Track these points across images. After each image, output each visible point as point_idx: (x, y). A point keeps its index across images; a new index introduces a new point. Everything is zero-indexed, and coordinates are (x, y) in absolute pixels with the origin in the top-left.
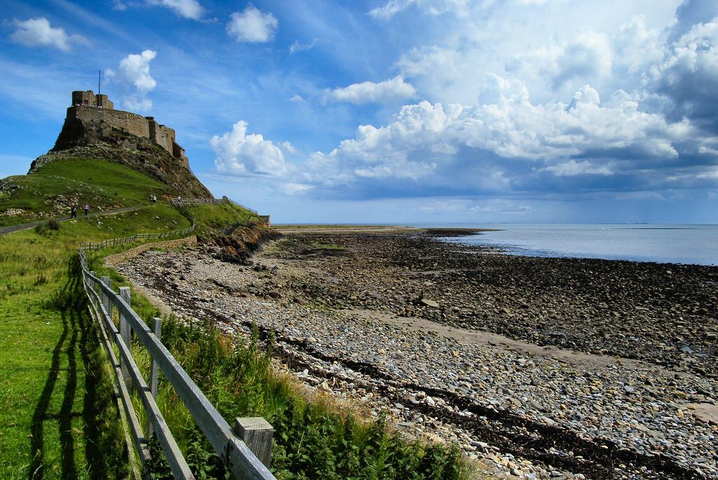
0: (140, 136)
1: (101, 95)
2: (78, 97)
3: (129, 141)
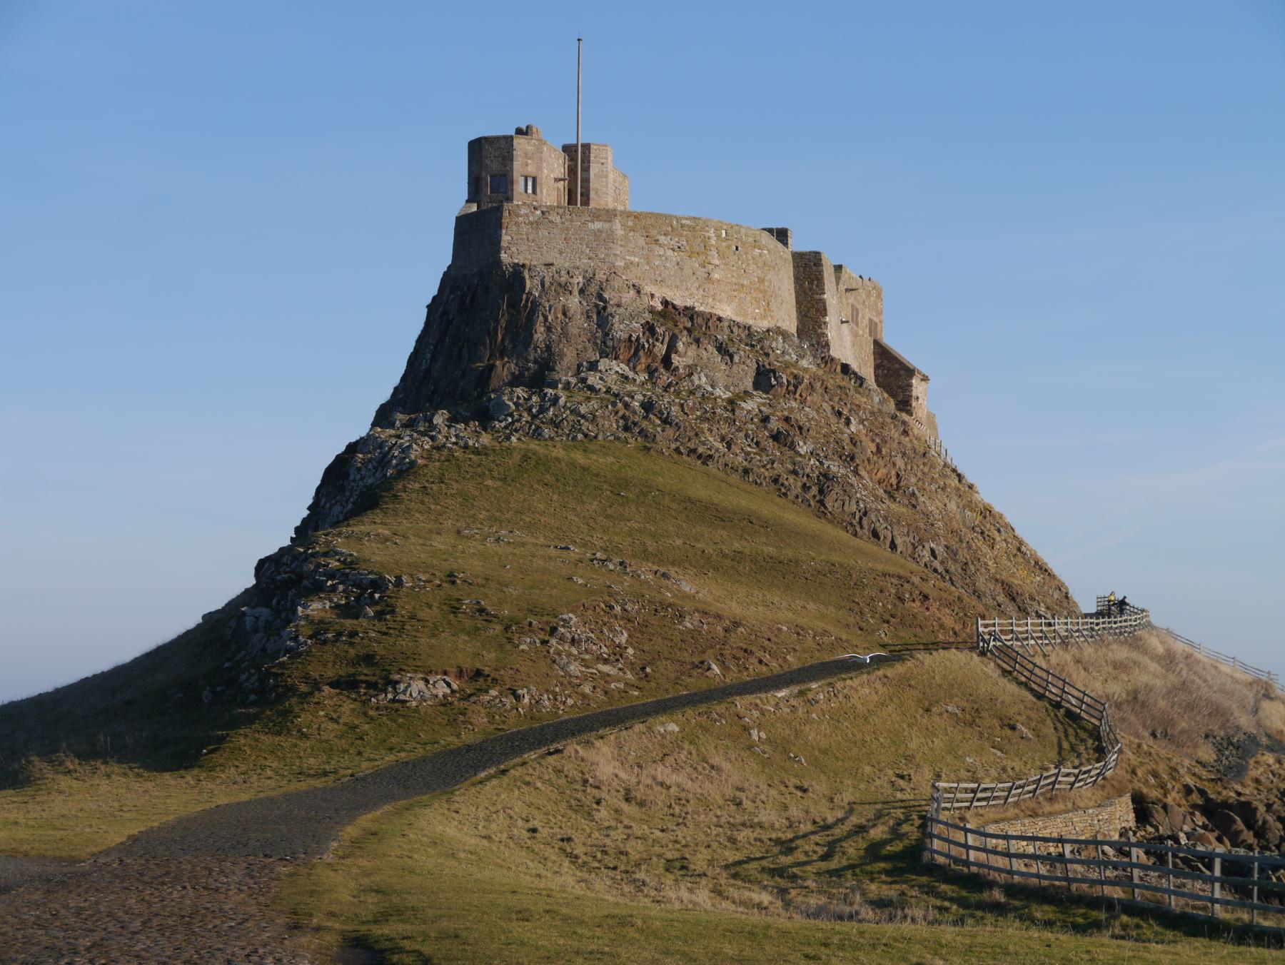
0: (762, 325)
1: (586, 147)
2: (493, 165)
3: (722, 349)
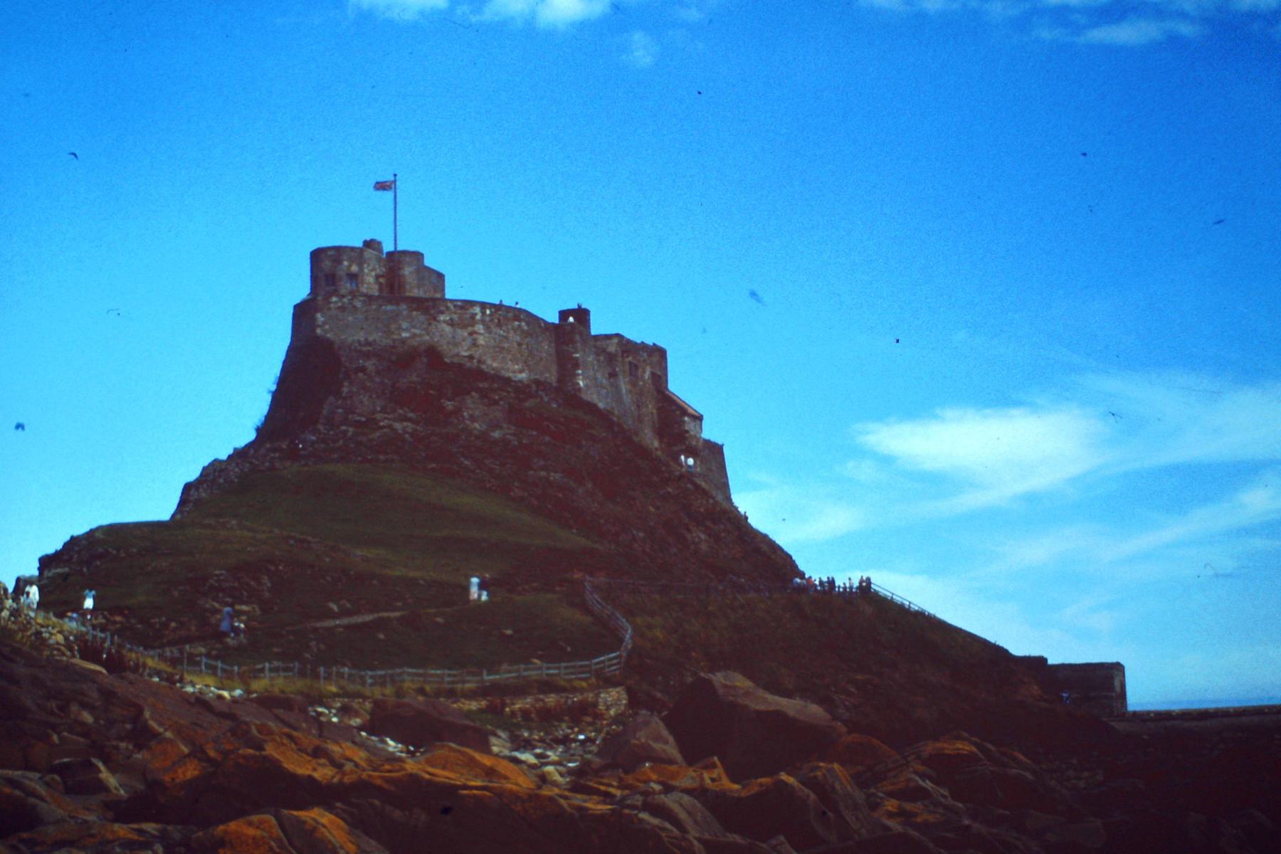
1: (404, 253)
3: (484, 394)
